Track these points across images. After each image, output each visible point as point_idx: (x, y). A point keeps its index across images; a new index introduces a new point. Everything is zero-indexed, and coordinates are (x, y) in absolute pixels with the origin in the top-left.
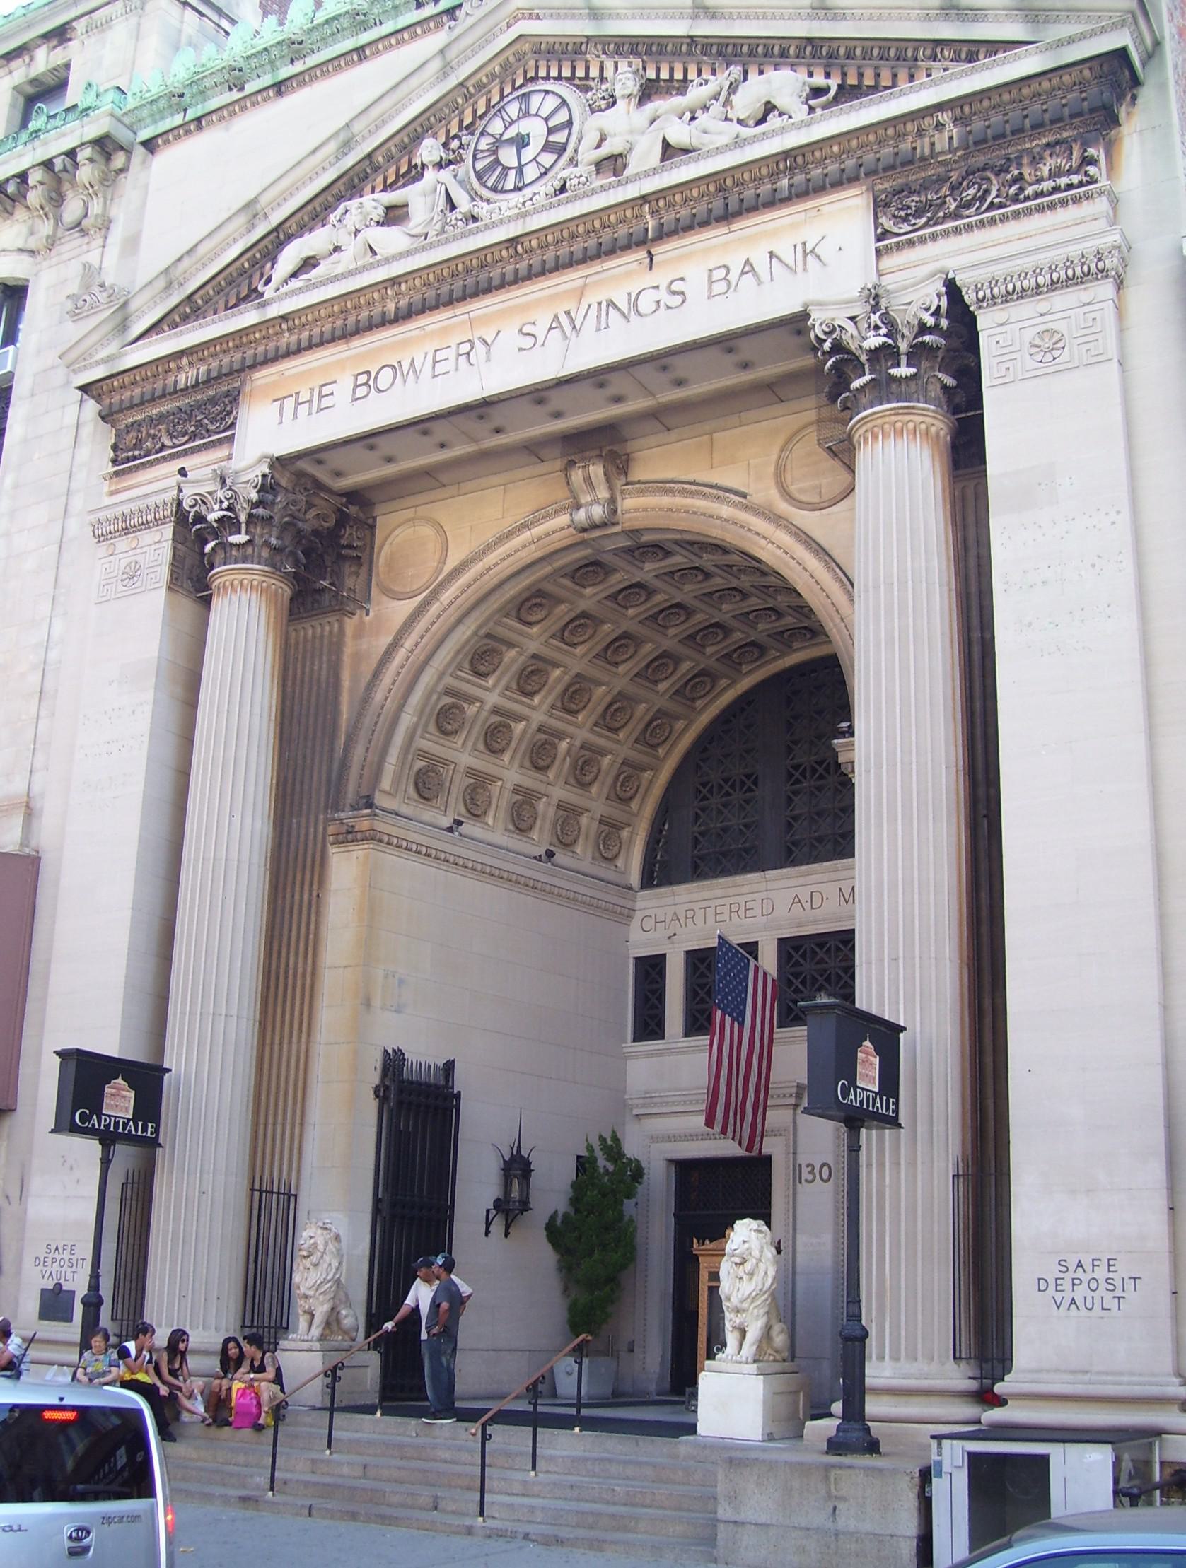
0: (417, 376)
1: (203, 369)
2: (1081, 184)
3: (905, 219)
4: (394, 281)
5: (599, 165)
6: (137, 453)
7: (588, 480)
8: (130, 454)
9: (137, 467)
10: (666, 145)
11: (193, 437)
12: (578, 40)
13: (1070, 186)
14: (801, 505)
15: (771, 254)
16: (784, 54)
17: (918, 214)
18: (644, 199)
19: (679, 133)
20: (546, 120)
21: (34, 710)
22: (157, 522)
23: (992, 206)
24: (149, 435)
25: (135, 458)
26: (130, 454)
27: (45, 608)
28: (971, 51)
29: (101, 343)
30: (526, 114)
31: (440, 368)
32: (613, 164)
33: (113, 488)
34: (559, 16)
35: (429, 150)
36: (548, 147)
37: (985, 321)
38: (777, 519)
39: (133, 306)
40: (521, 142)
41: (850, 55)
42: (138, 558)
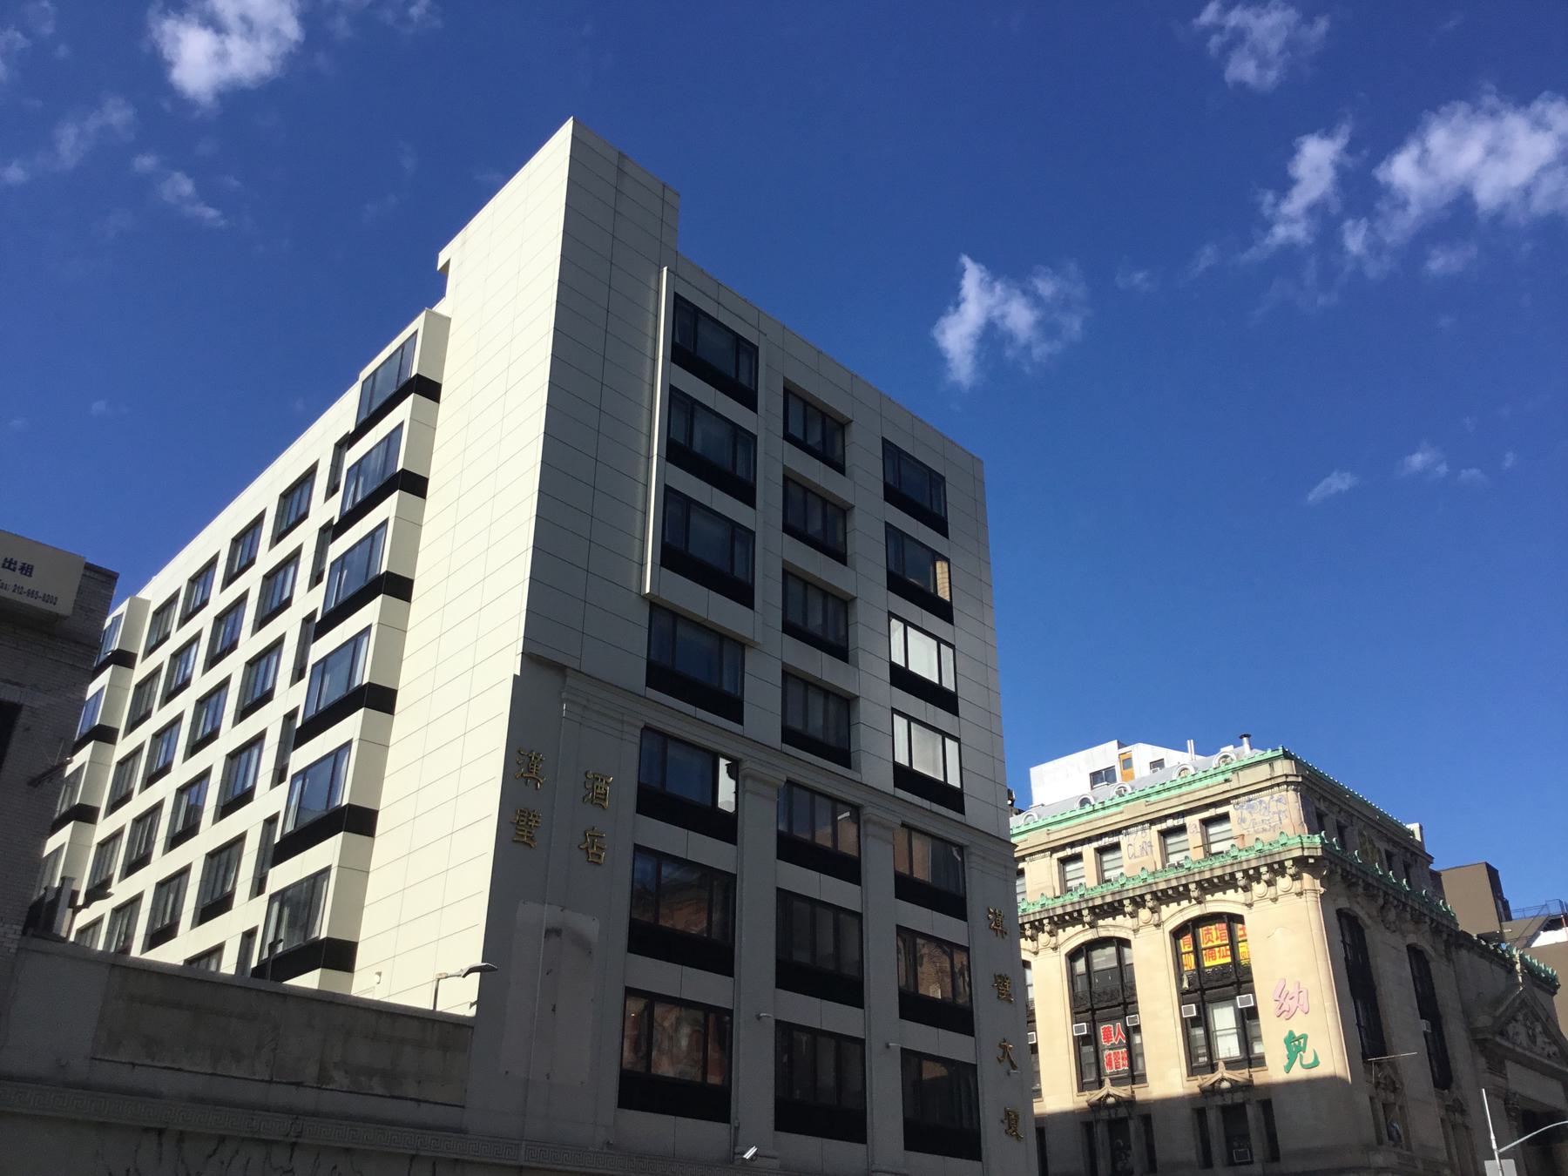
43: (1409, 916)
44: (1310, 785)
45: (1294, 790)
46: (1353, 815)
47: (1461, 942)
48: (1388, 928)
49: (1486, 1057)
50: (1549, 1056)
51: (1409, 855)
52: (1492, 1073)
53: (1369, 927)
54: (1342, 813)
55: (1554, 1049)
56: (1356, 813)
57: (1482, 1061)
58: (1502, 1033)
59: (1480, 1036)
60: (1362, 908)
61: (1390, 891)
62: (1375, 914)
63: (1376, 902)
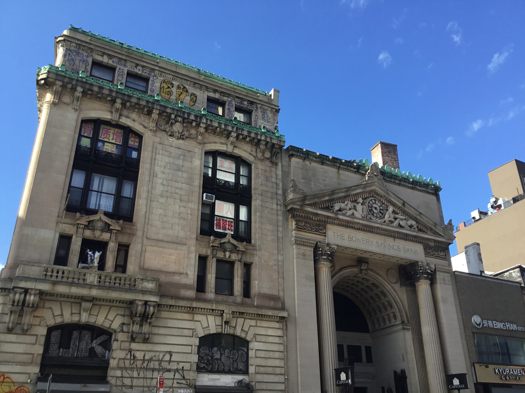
0: (360, 242)
1: (319, 219)
2: (444, 258)
3: (427, 253)
4: (358, 223)
5: (390, 221)
6: (303, 228)
7: (365, 266)
8: (301, 227)
9: (303, 231)
10: (399, 223)
11: (316, 231)
12: (382, 195)
13: (444, 258)
14: (391, 282)
15: (411, 249)
16: (412, 217)
17: (429, 253)
18: (397, 232)
19: (402, 223)
20: (379, 207)
21: (277, 276)
22: (312, 247)
23: (437, 256)
24: (305, 225)
25: (302, 229)
26: (301, 227)
27: (276, 252)
28: (436, 233)
29: (299, 201)
30: (375, 203)
31: (364, 242)
32: (391, 222)
33: (297, 233)
34: (381, 190)
35: (360, 200)
36: (380, 212)
37: (438, 273)
38: (389, 284)
39: (308, 197)
40: (376, 208)
41: (420, 223)
42: (306, 252)
43: (202, 130)
44: (79, 42)
45: (61, 46)
46: (153, 70)
47: (291, 153)
48: (171, 136)
49: (296, 221)
50: (400, 226)
51: (245, 103)
52: (298, 230)
53: (142, 133)
54: (139, 67)
55: (412, 222)
56: (157, 68)
57: (293, 224)
58: (328, 208)
59: (289, 208)
60: (134, 120)
61: (169, 111)
62: (152, 125)
63: (151, 117)
